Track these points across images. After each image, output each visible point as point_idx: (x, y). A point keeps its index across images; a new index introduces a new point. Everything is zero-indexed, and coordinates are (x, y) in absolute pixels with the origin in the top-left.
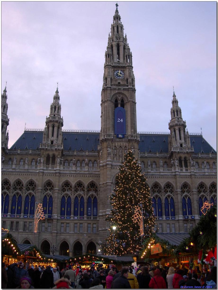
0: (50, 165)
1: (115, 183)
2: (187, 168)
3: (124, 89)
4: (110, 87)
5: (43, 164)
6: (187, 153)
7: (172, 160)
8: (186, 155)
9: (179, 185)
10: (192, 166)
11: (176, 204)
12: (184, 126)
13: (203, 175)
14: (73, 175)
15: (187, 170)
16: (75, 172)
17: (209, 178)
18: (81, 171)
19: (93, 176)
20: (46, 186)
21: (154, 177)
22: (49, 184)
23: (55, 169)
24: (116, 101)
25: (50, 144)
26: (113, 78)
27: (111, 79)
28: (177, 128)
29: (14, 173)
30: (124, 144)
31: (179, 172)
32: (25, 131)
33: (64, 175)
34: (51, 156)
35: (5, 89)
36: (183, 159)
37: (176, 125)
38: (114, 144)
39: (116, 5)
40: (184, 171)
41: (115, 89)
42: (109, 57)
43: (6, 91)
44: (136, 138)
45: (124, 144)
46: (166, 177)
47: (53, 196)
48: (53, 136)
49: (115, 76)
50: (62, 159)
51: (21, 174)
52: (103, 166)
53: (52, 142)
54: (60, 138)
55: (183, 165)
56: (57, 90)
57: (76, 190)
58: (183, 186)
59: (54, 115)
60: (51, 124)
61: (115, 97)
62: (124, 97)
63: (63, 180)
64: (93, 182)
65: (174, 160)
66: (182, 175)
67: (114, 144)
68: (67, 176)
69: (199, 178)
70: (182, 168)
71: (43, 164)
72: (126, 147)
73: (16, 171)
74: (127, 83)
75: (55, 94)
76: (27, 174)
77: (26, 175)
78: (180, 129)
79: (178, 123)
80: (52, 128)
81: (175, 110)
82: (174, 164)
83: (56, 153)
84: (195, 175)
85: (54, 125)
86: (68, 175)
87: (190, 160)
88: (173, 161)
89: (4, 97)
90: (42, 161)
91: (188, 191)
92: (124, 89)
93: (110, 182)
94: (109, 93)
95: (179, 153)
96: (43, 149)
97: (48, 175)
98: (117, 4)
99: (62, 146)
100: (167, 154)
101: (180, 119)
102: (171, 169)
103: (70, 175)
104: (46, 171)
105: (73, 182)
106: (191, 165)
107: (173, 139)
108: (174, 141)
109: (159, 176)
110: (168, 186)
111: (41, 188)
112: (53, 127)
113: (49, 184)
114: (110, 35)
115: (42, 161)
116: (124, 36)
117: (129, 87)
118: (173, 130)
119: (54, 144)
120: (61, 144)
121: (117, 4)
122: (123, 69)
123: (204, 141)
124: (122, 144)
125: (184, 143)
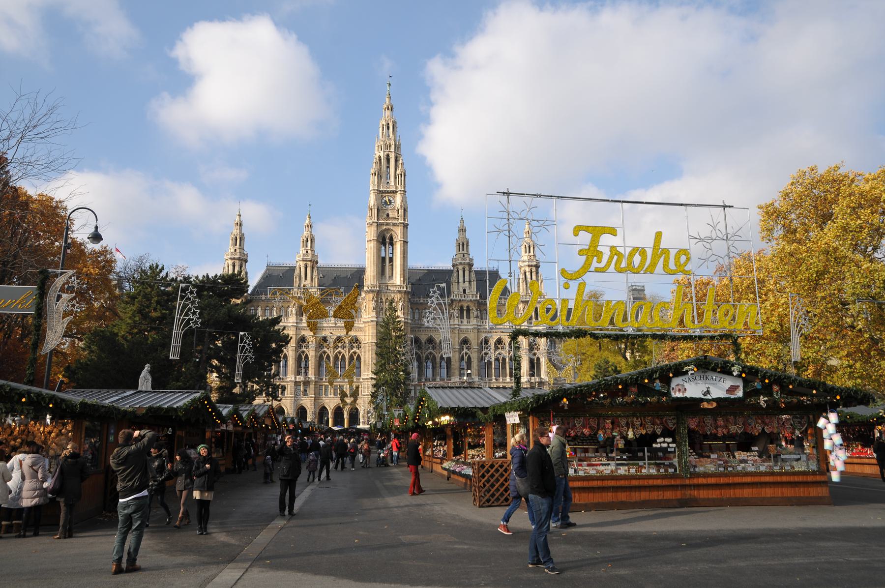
3: (394, 225)
4: (377, 223)
6: (471, 301)
8: (469, 303)
11: (452, 364)
12: (471, 265)
15: (468, 322)
26: (380, 208)
27: (378, 209)
28: (460, 267)
31: (459, 325)
32: (268, 266)
36: (465, 308)
37: (461, 264)
40: (465, 322)
49: (383, 205)
52: (368, 322)
55: (465, 317)
57: (336, 347)
58: (463, 341)
59: (307, 252)
60: (302, 264)
62: (393, 233)
65: (453, 309)
67: (380, 296)
81: (461, 243)
84: (479, 329)
88: (452, 311)
91: (469, 348)
92: (394, 225)
95: (460, 300)
101: (465, 255)
112: (306, 268)
115: (294, 312)
117: (400, 221)
118: (456, 270)
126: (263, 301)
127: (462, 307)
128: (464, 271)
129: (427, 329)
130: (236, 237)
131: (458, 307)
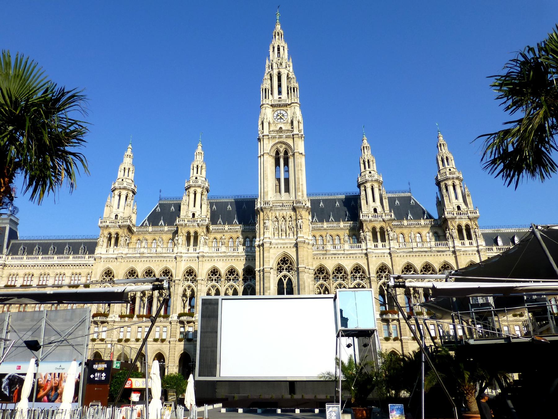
1: (277, 268)
2: (384, 243)
4: (268, 135)
5: (181, 246)
7: (361, 231)
8: (383, 224)
9: (374, 269)
10: (391, 240)
13: (410, 252)
15: (384, 246)
16: (224, 255)
17: (419, 256)
18: (233, 253)
19: (249, 260)
20: (186, 276)
21: (335, 258)
24: (277, 153)
29: (143, 260)
30: (288, 213)
33: (210, 259)
34: (192, 234)
36: (378, 230)
38: (273, 215)
41: (274, 137)
42: (294, 91)
44: (304, 204)
45: (288, 213)
46: (353, 257)
48: (194, 206)
51: (151, 260)
53: (194, 215)
54: (204, 207)
59: (196, 178)
61: (275, 147)
64: (249, 267)
66: (378, 253)
68: (214, 260)
69: (403, 256)
70: (377, 243)
71: (182, 245)
72: (291, 217)
73: (145, 257)
74: (292, 128)
76: (159, 259)
77: (158, 261)
78: (372, 186)
79: (369, 178)
80: (194, 195)
82: (364, 237)
83: (199, 230)
85: (195, 192)
86: (216, 259)
87: (388, 232)
90: (180, 241)
93: (268, 268)
94: (267, 144)
95: (371, 221)
96: (182, 225)
97: (189, 260)
100: (356, 223)
102: (360, 245)
103: (219, 259)
104: (187, 255)
105: (223, 268)
106: (390, 238)
107: (363, 202)
108: (364, 205)
109: (343, 256)
110: (357, 270)
112: (195, 194)
113: (190, 273)
117: (295, 133)
119: (196, 217)
120: (205, 217)
122: (285, 108)
123: (413, 202)
124: (285, 213)
125: (379, 207)
126: (149, 233)
127: (374, 229)
128: (372, 189)
129: (334, 256)
131: (370, 228)
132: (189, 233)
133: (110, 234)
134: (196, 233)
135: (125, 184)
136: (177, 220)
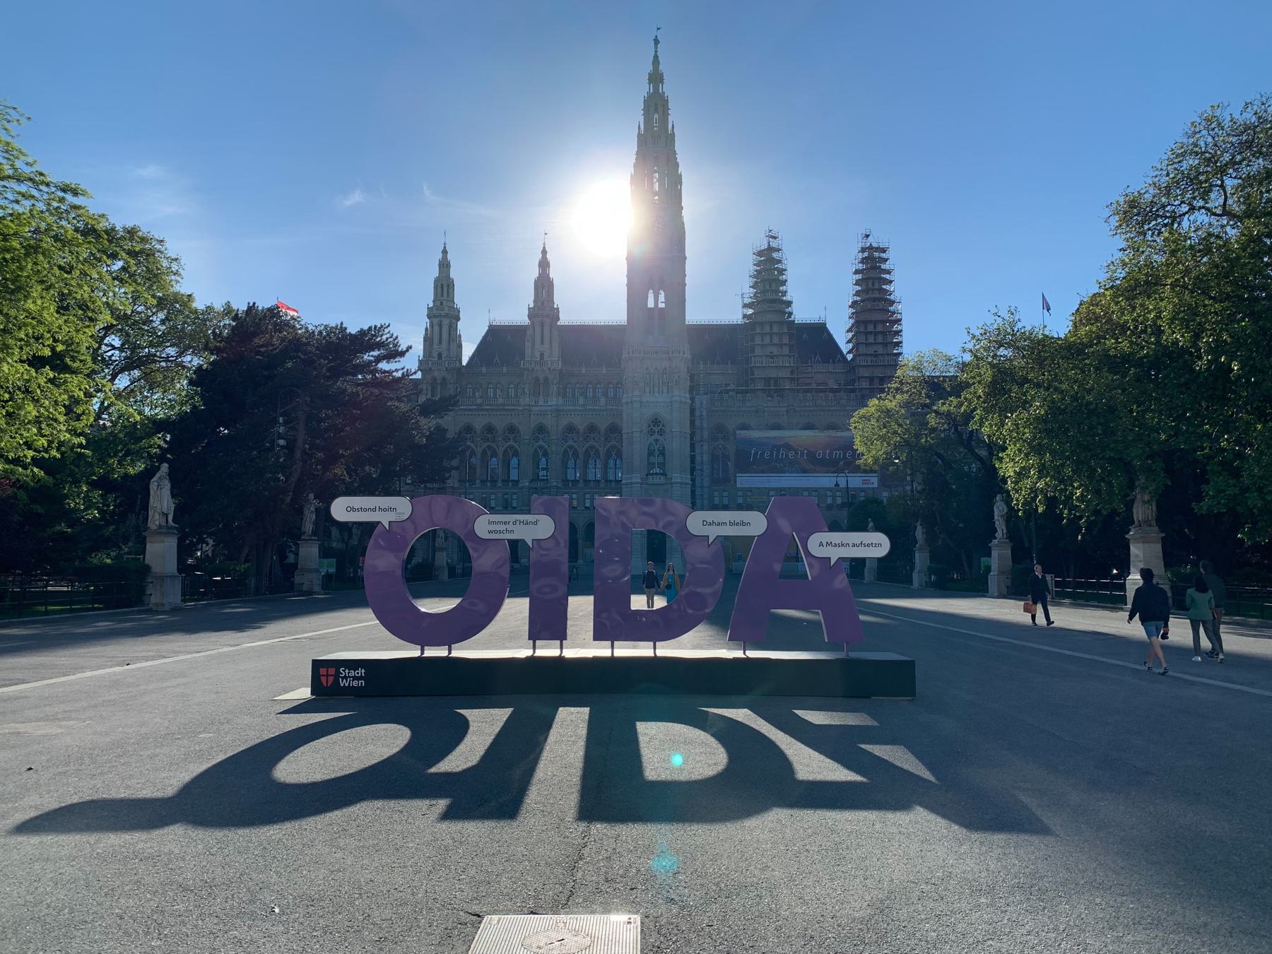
0: (541, 397)
14: (580, 413)
22: (541, 429)
23: (549, 404)
25: (539, 359)
35: (445, 247)
39: (654, 40)
43: (447, 253)
47: (548, 450)
48: (542, 343)
50: (561, 386)
52: (627, 403)
56: (544, 248)
63: (564, 422)
75: (541, 256)
86: (573, 413)
89: (445, 265)
98: (656, 37)
99: (560, 362)
103: (576, 413)
104: (536, 408)
111: (528, 438)
114: (642, 127)
116: (670, 127)
119: (545, 359)
121: (656, 37)
130: (442, 285)
132: (537, 379)
133: (435, 379)
134: (546, 379)
135: (446, 310)
136: (522, 363)
